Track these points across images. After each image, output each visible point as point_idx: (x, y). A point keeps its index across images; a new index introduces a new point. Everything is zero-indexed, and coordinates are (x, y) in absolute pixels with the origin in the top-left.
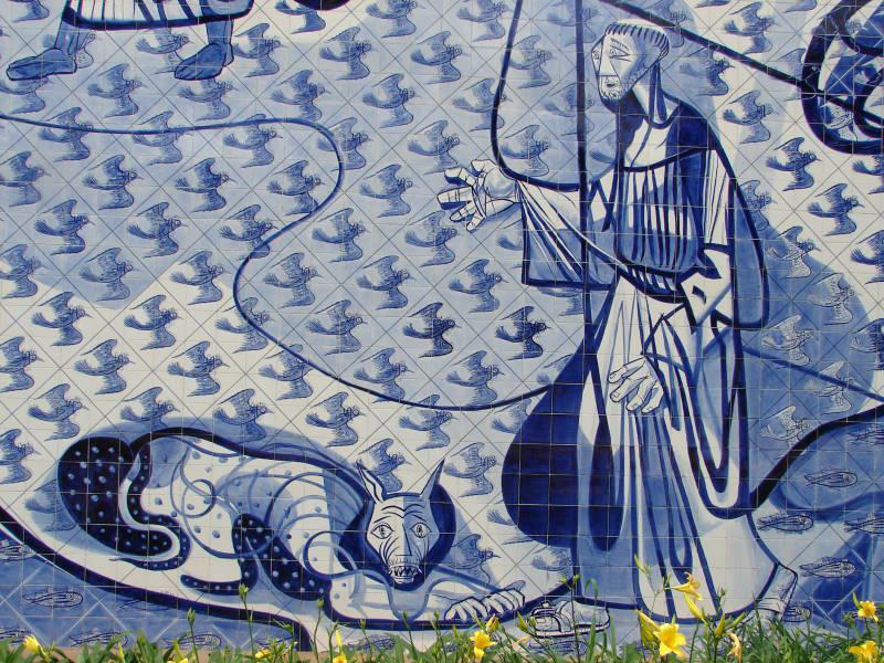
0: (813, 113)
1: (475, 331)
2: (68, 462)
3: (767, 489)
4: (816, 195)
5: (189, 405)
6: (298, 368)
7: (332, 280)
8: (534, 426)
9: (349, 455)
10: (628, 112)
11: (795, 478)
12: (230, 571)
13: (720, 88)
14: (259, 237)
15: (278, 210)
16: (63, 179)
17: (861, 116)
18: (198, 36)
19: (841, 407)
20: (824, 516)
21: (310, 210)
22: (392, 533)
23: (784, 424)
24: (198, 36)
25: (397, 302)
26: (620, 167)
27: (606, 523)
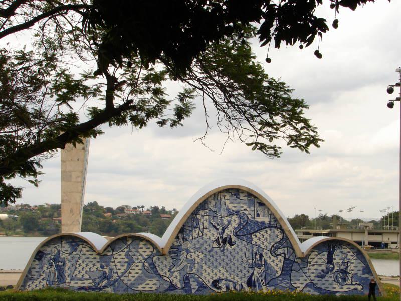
0: (271, 254)
1: (244, 272)
2: (213, 282)
3: (268, 284)
4: (271, 260)
5: (222, 277)
6: (230, 275)
7: (233, 268)
8: (248, 279)
9: (234, 281)
10: (256, 254)
11: (270, 283)
12: (225, 290)
13: (263, 252)
14: (227, 264)
15: (229, 262)
16: (212, 260)
17: (275, 254)
18: (222, 248)
19: (273, 277)
20: (272, 286)
21: (231, 262)
22: (238, 288)
23: (269, 279)
24: (222, 248)
25: (238, 269)
26: (255, 258)
27: (255, 287)
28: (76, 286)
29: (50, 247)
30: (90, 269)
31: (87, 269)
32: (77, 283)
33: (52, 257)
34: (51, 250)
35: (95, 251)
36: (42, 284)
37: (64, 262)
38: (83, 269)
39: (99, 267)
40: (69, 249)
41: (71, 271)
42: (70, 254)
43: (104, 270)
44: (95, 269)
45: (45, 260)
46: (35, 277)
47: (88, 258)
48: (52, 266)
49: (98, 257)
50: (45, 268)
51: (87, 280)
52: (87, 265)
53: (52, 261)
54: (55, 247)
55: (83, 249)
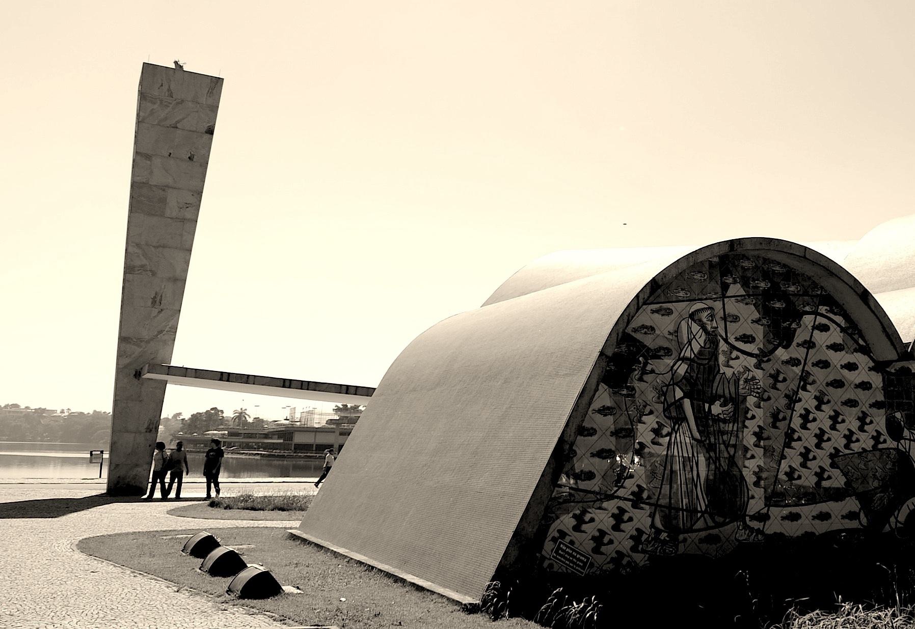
28: (793, 529)
29: (669, 312)
30: (849, 437)
31: (837, 440)
32: (794, 517)
33: (682, 369)
34: (677, 331)
35: (865, 350)
36: (627, 527)
37: (737, 401)
38: (820, 437)
39: (883, 430)
40: (759, 332)
41: (769, 452)
42: (763, 357)
43: (904, 445)
44: (865, 442)
45: (646, 390)
46: (594, 485)
47: (838, 384)
48: (680, 419)
49: (876, 380)
50: (644, 433)
51: (837, 495)
52: (835, 419)
53: (679, 394)
54: (692, 316)
55: (818, 336)
